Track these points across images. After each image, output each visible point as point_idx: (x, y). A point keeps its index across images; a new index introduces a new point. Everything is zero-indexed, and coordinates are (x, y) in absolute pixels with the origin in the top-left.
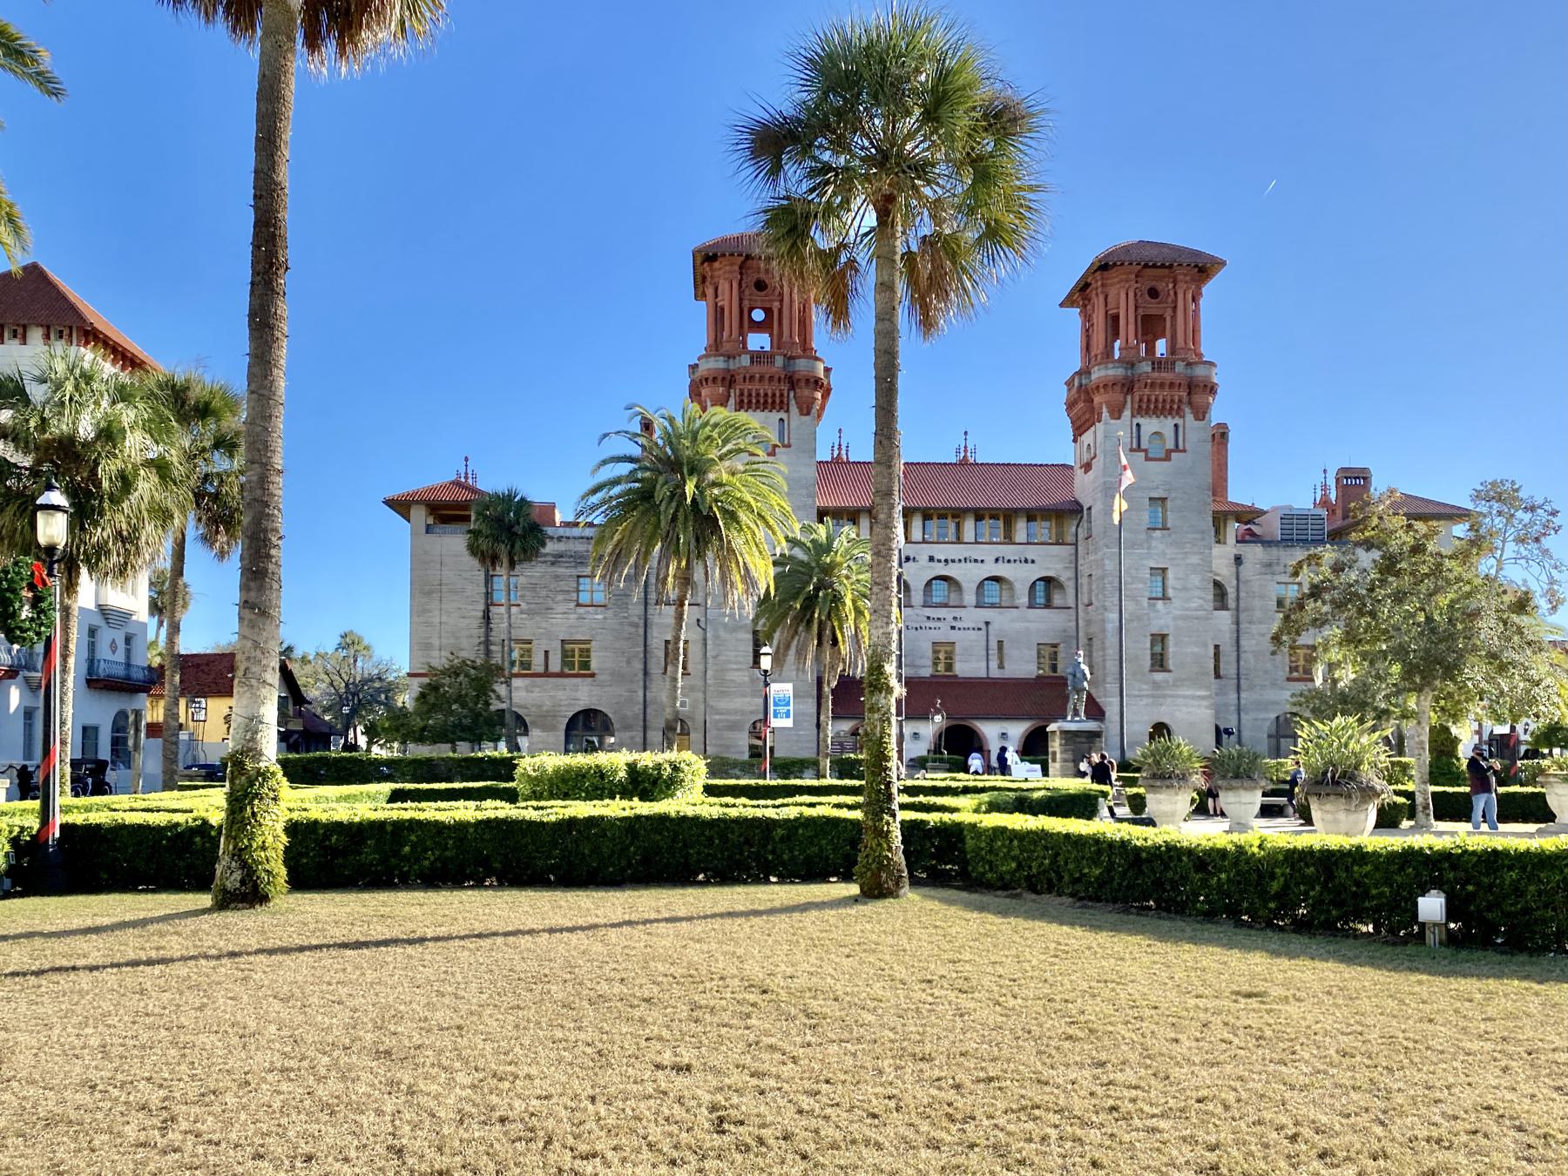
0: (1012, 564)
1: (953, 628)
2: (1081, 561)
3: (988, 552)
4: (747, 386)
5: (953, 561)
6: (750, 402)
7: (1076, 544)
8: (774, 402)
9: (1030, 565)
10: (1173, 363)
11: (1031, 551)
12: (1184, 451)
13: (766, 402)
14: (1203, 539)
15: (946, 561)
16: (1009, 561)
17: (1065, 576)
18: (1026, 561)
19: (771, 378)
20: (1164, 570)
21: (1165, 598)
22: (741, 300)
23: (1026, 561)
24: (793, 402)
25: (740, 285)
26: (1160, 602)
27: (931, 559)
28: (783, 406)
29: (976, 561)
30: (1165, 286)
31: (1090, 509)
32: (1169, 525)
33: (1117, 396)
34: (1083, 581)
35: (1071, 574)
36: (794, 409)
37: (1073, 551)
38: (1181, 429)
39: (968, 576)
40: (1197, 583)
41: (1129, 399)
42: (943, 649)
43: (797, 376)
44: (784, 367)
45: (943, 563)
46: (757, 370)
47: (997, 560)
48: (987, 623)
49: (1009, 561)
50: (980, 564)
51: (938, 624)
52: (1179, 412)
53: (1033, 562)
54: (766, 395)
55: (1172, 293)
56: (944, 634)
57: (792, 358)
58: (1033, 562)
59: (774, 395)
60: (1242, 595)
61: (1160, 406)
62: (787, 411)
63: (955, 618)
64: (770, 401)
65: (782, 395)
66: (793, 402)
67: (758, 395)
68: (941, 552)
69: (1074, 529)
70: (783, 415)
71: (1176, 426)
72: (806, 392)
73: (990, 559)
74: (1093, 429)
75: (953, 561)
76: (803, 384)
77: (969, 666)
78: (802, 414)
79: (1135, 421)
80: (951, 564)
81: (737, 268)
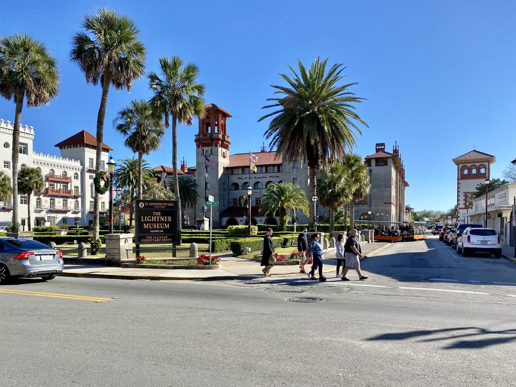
0: (274, 178)
4: (203, 142)
5: (260, 178)
6: (204, 145)
9: (278, 178)
11: (278, 174)
13: (207, 145)
14: (306, 170)
15: (258, 178)
18: (277, 177)
19: (207, 139)
27: (255, 178)
28: (211, 145)
29: (265, 177)
36: (214, 146)
40: (304, 181)
42: (259, 199)
43: (213, 138)
44: (210, 136)
46: (204, 138)
47: (270, 177)
54: (207, 143)
57: (212, 134)
58: (279, 177)
59: (208, 143)
62: (212, 146)
63: (261, 192)
66: (213, 144)
70: (212, 148)
72: (216, 141)
75: (260, 178)
80: (260, 179)
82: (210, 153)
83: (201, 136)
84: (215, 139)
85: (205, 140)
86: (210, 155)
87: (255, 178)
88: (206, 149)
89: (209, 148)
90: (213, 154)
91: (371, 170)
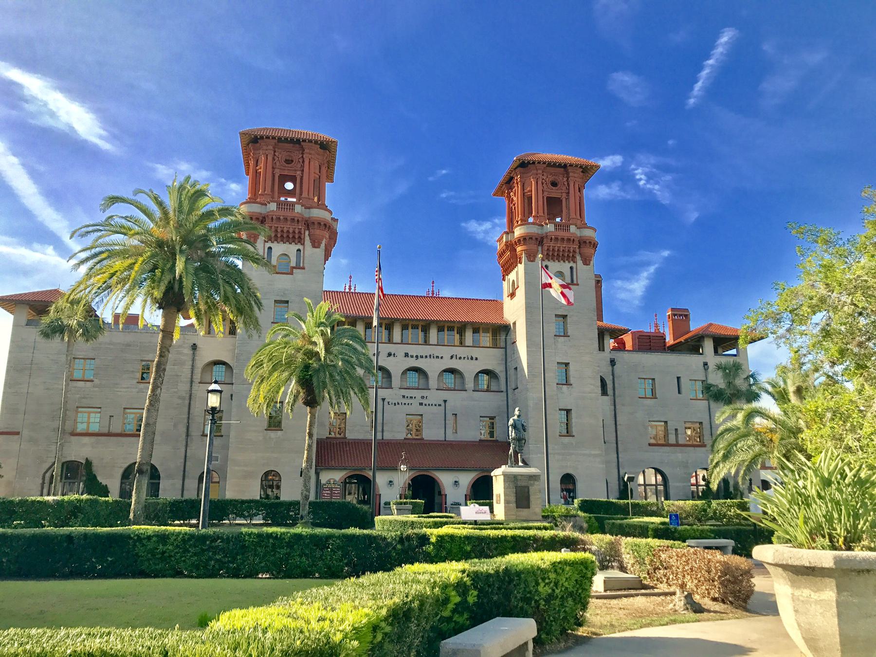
1: (421, 404)
2: (509, 360)
3: (446, 351)
5: (422, 357)
7: (506, 348)
8: (294, 237)
9: (474, 361)
10: (568, 226)
11: (475, 352)
12: (577, 285)
15: (417, 357)
16: (460, 358)
17: (499, 369)
18: (472, 358)
20: (567, 364)
21: (567, 383)
22: (273, 168)
23: (472, 358)
24: (307, 238)
25: (274, 159)
26: (565, 387)
27: (406, 355)
28: (301, 241)
29: (437, 357)
30: (561, 179)
31: (514, 324)
32: (569, 334)
33: (533, 247)
34: (511, 372)
35: (503, 368)
37: (504, 353)
38: (575, 270)
39: (433, 368)
41: (540, 248)
45: (415, 358)
46: (282, 213)
47: (452, 357)
48: (445, 401)
49: (460, 358)
50: (439, 360)
51: (410, 401)
52: (574, 260)
53: (476, 359)
54: (288, 231)
55: (566, 183)
56: (415, 408)
58: (476, 359)
59: (294, 232)
60: (616, 385)
61: (561, 254)
62: (303, 244)
63: (423, 397)
64: (291, 236)
65: (300, 233)
66: (307, 238)
67: (282, 231)
68: (413, 350)
69: (503, 337)
70: (299, 247)
71: (571, 268)
72: (318, 232)
73: (447, 357)
74: (516, 269)
75: (422, 357)
76: (316, 226)
77: (432, 433)
78: (314, 246)
79: (544, 264)
81: (271, 147)
82: (293, 264)
83: (273, 206)
84: (319, 224)
85: (286, 219)
86: (294, 268)
87: (406, 355)
88: (279, 248)
89: (291, 249)
90: (303, 268)
91: (705, 364)
